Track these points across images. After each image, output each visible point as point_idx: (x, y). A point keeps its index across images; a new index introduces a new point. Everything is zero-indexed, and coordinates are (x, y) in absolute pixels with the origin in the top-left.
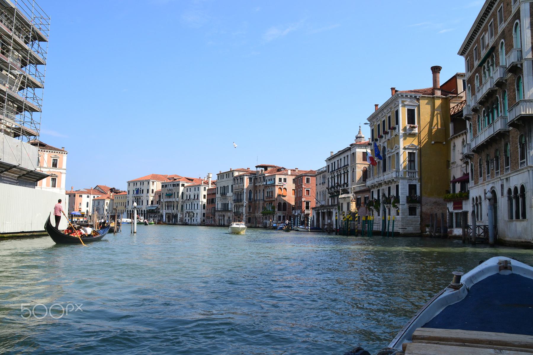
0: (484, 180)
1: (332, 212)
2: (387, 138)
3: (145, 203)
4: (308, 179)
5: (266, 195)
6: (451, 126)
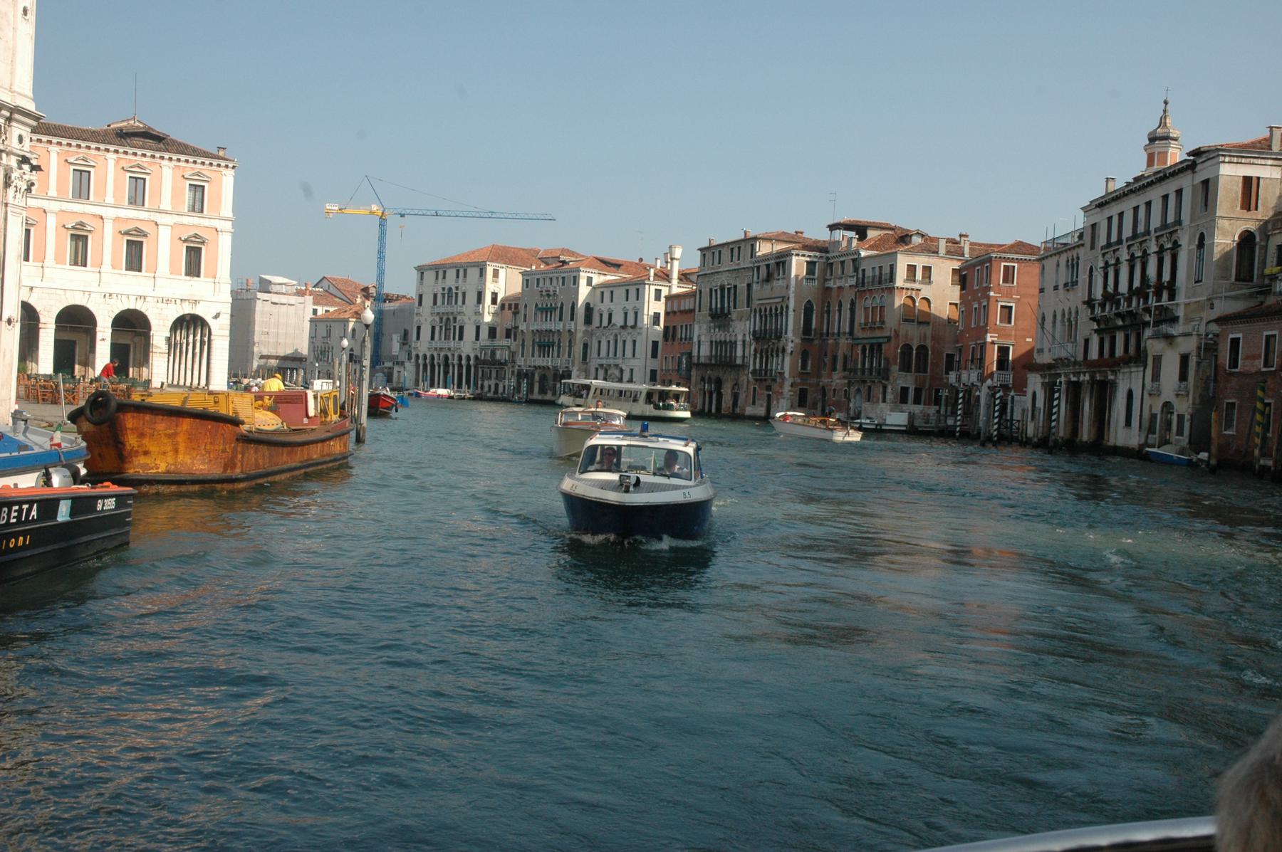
1: (1114, 385)
3: (469, 333)
4: (1008, 273)
5: (860, 318)
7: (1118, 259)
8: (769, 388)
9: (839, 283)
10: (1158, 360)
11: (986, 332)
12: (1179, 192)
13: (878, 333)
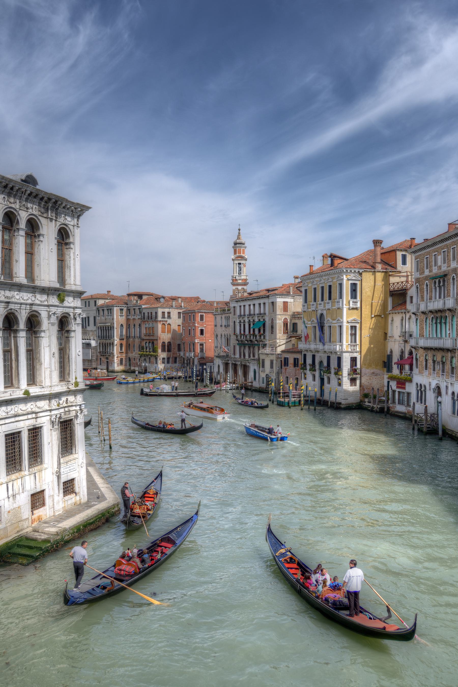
0: (430, 374)
2: (327, 307)
4: (202, 317)
5: (144, 331)
6: (390, 300)
7: (244, 321)
8: (107, 358)
9: (133, 317)
10: (263, 361)
11: (195, 339)
12: (264, 304)
13: (151, 338)
